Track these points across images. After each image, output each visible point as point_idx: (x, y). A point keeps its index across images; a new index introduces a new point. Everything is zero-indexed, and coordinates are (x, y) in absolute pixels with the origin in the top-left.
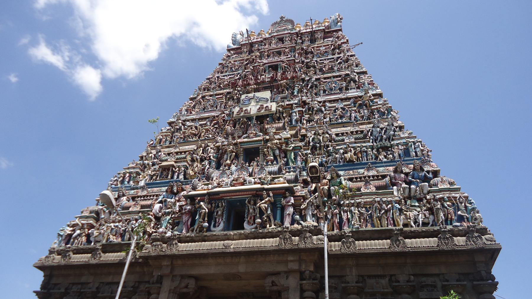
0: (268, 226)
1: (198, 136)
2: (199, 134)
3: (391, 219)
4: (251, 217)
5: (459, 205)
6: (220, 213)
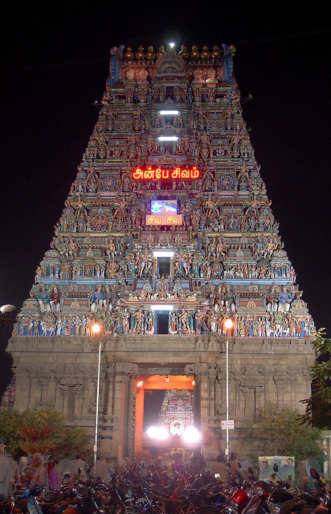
0: (186, 333)
1: (105, 226)
2: (106, 225)
3: (264, 331)
4: (173, 326)
5: (305, 323)
6: (151, 320)
